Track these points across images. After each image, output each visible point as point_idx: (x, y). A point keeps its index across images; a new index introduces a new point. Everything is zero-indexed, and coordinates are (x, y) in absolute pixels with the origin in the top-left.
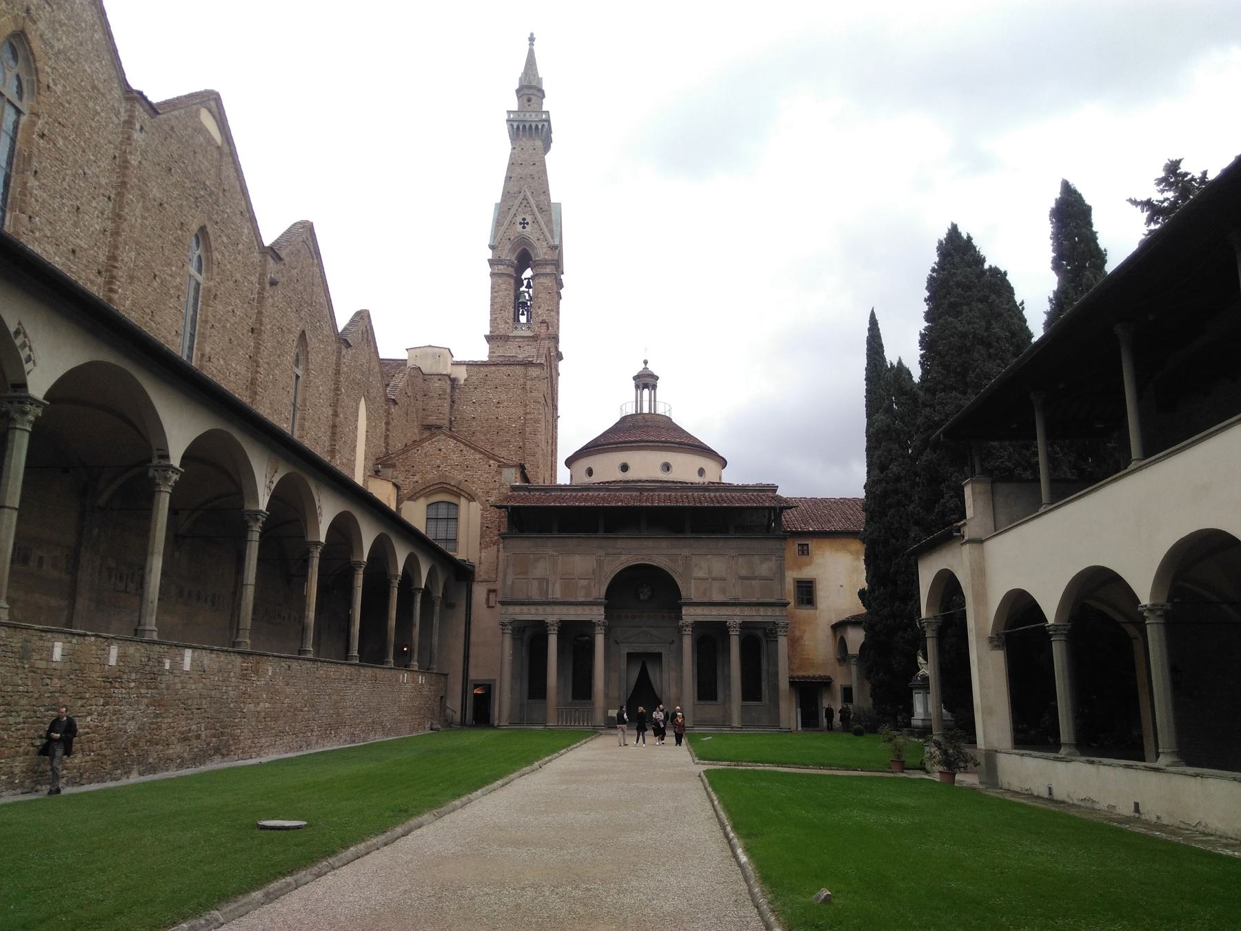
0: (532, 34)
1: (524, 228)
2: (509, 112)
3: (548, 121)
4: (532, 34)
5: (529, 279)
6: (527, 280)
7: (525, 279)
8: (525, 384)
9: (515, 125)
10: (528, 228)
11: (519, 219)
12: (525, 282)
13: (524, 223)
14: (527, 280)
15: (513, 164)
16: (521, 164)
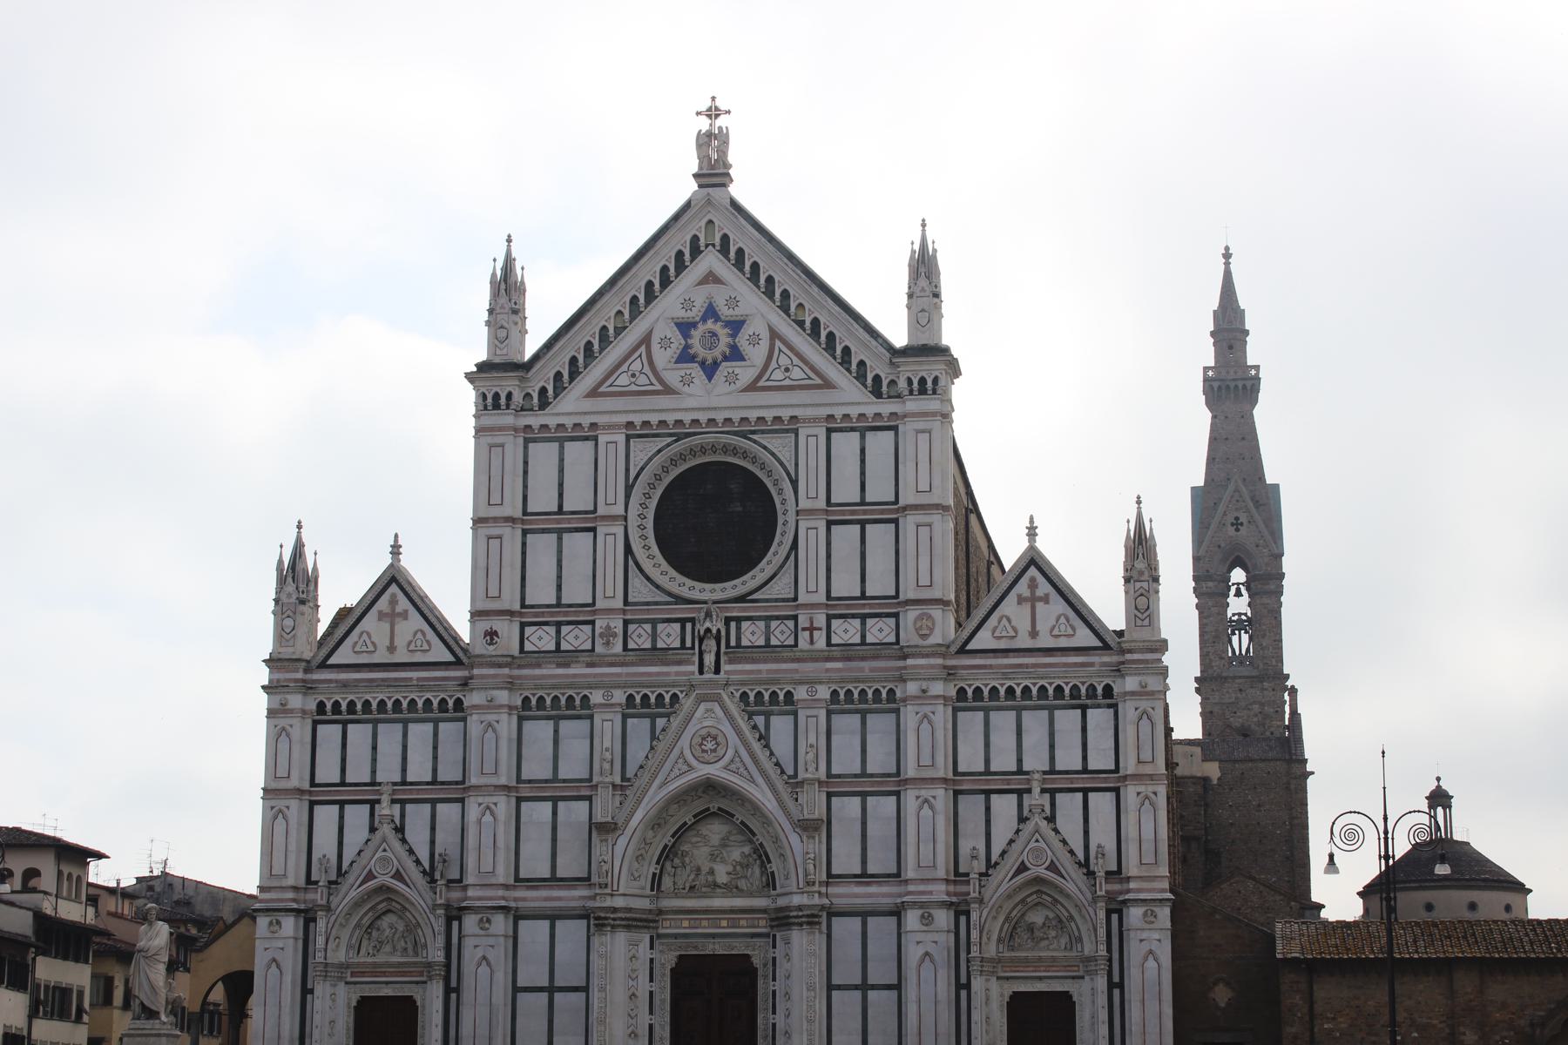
0: (1227, 248)
1: (1237, 530)
2: (1206, 369)
3: (1257, 379)
4: (1227, 248)
5: (1238, 584)
6: (1236, 586)
7: (1233, 584)
8: (1289, 783)
9: (1216, 385)
10: (1243, 530)
11: (1230, 519)
12: (1233, 590)
13: (1237, 524)
14: (1236, 586)
15: (1215, 439)
16: (1227, 439)
